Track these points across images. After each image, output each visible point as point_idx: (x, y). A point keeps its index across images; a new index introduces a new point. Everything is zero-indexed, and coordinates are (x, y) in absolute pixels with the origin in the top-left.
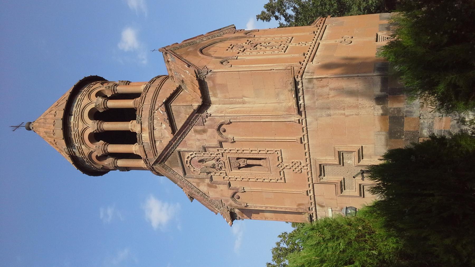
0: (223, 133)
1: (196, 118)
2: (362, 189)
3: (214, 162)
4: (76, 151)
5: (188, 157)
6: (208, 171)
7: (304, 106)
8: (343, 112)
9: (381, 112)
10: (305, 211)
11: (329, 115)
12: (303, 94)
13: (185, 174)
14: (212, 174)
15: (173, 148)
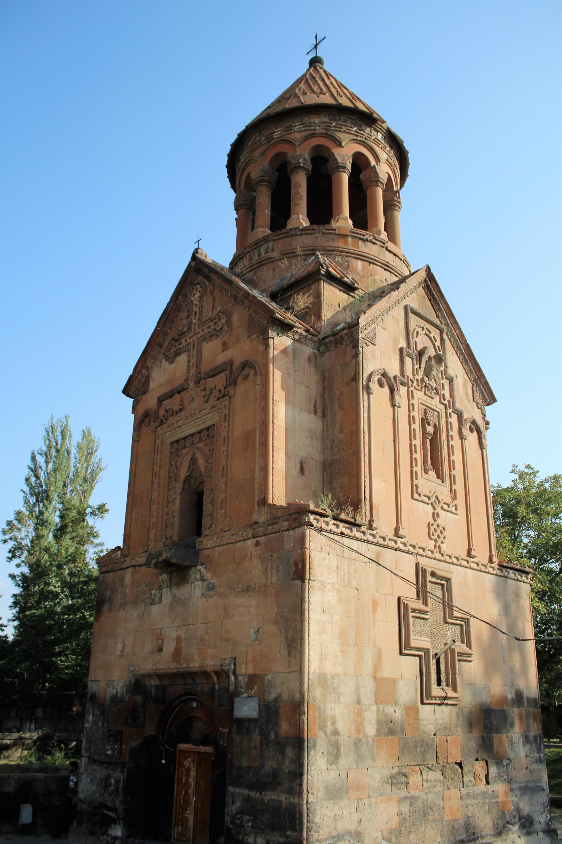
1: (483, 396)
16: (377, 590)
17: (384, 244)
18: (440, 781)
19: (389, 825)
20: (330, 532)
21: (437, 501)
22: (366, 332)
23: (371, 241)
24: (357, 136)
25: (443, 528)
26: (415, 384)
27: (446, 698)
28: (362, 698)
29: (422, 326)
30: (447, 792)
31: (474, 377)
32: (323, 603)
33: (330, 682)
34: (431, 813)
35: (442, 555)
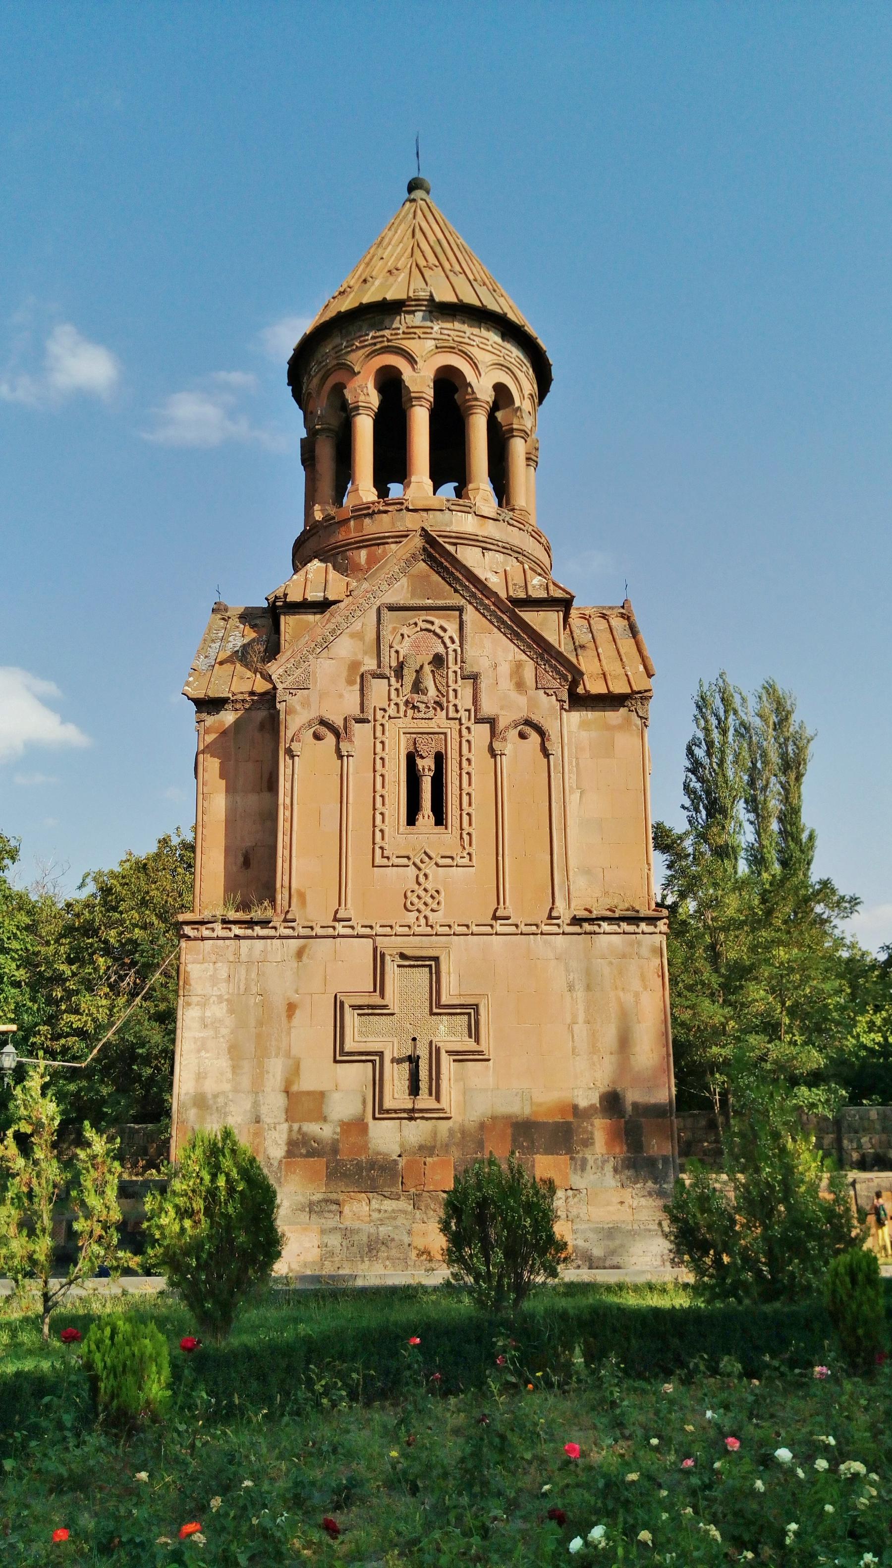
0: (515, 732)
1: (558, 672)
2: (364, 1058)
3: (432, 692)
4: (418, 318)
5: (445, 630)
6: (405, 671)
7: (595, 933)
8: (581, 1018)
9: (583, 1103)
10: (279, 910)
11: (571, 988)
12: (624, 933)
13: (392, 608)
14: (393, 680)
15: (474, 595)
16: (297, 992)
17: (402, 504)
18: (405, 1212)
19: (302, 1258)
20: (218, 938)
21: (426, 859)
22: (290, 679)
23: (380, 512)
24: (375, 344)
25: (437, 892)
26: (392, 711)
27: (413, 1110)
28: (263, 1117)
29: (412, 622)
30: (418, 1227)
31: (536, 653)
32: (203, 1019)
33: (211, 1102)
34: (383, 1248)
35: (432, 927)
